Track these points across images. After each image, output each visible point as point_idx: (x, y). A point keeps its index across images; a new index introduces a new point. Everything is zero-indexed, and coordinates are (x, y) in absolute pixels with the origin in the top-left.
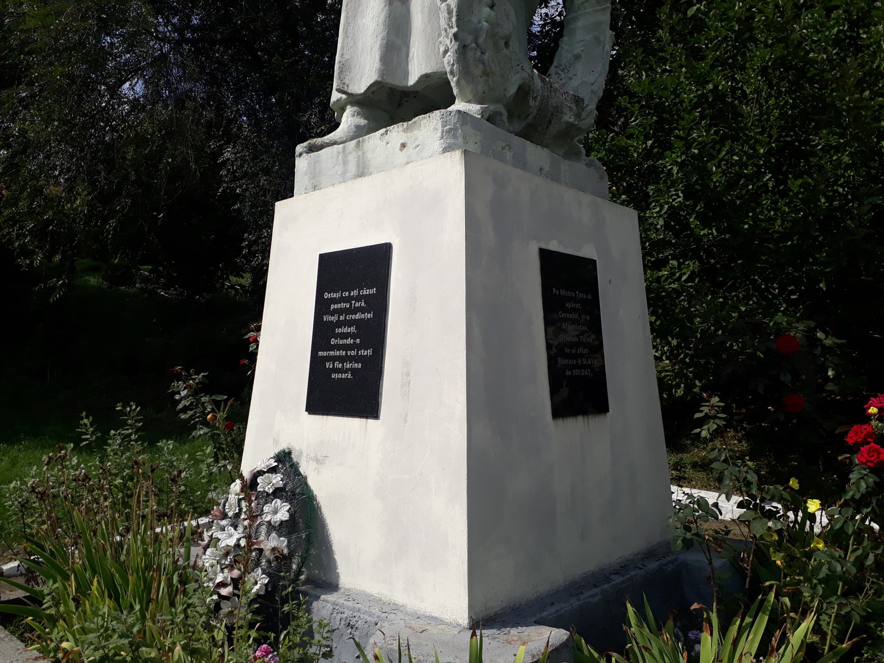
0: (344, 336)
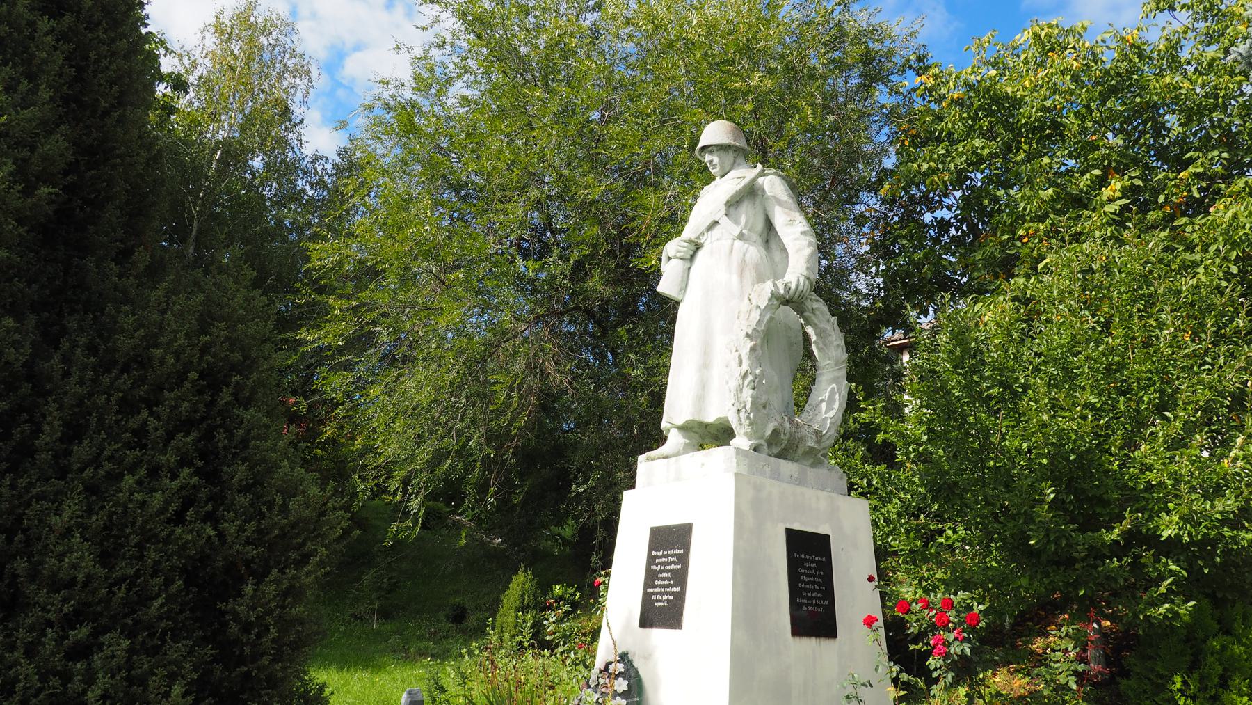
0: (663, 579)
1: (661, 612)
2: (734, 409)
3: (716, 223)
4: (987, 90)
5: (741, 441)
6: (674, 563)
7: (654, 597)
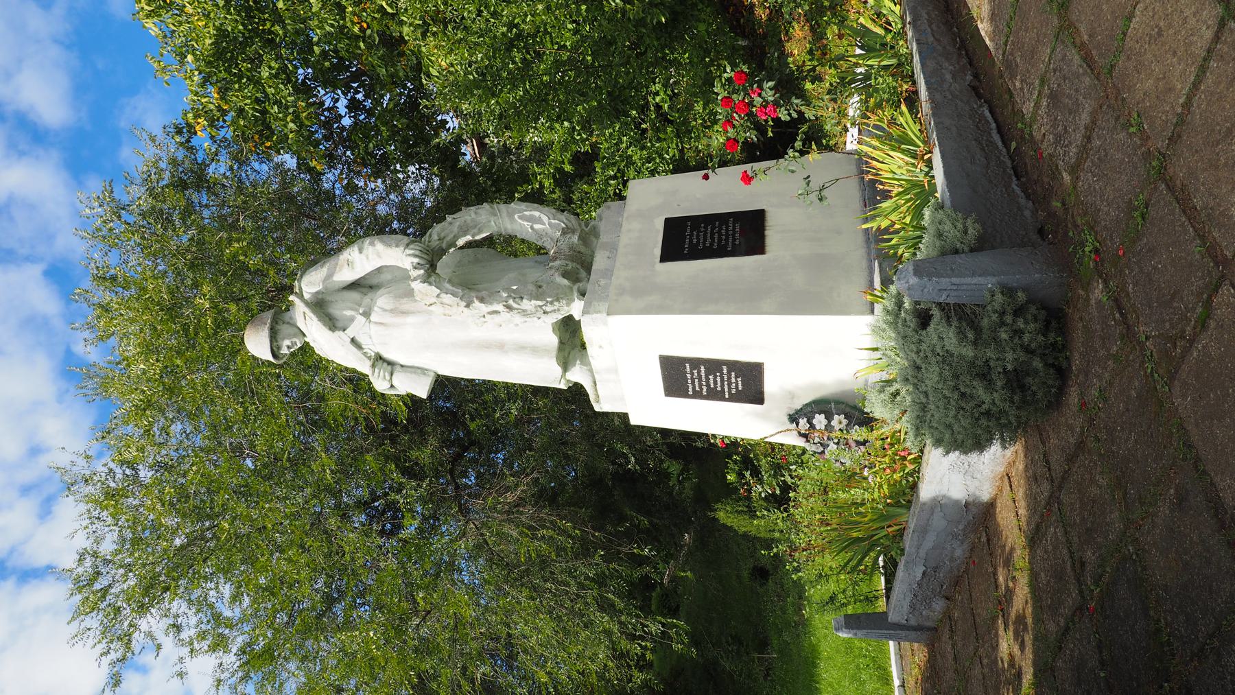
1: (747, 383)
2: (544, 317)
3: (353, 341)
4: (209, 64)
5: (576, 308)
6: (699, 372)
7: (734, 391)
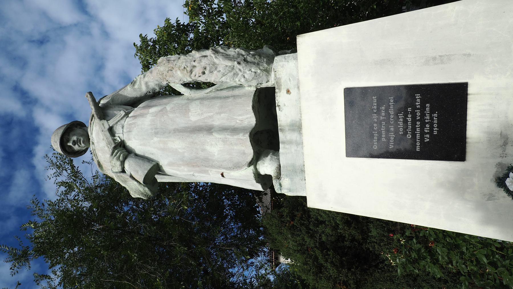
2: (243, 64)
